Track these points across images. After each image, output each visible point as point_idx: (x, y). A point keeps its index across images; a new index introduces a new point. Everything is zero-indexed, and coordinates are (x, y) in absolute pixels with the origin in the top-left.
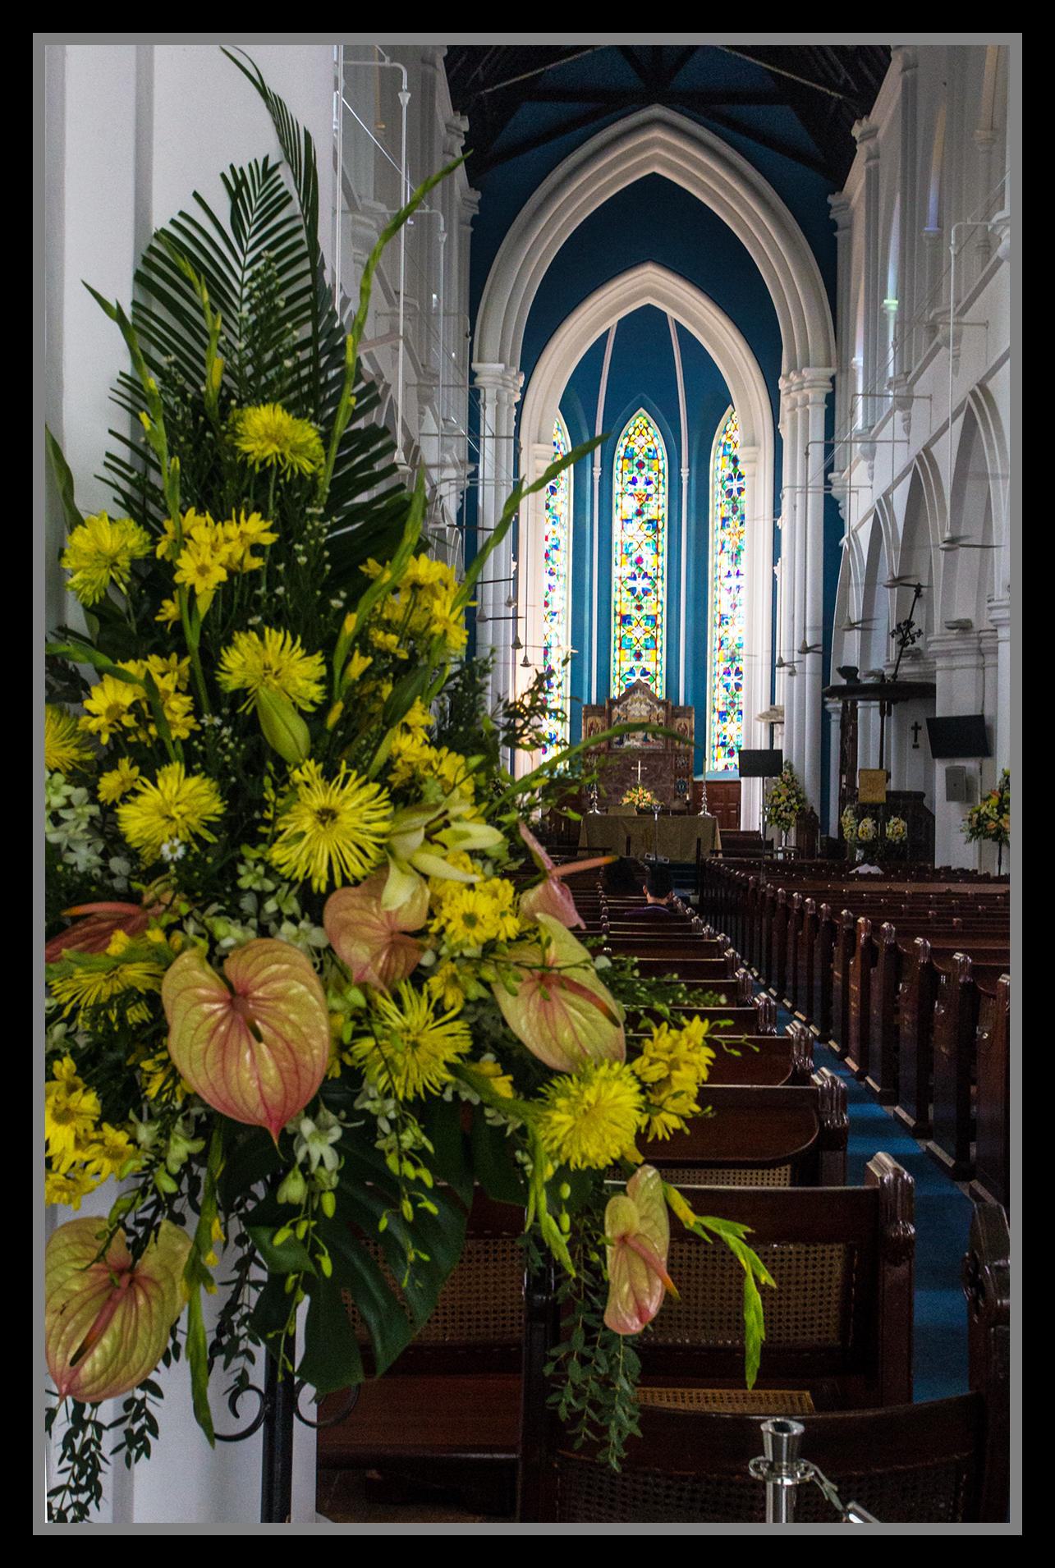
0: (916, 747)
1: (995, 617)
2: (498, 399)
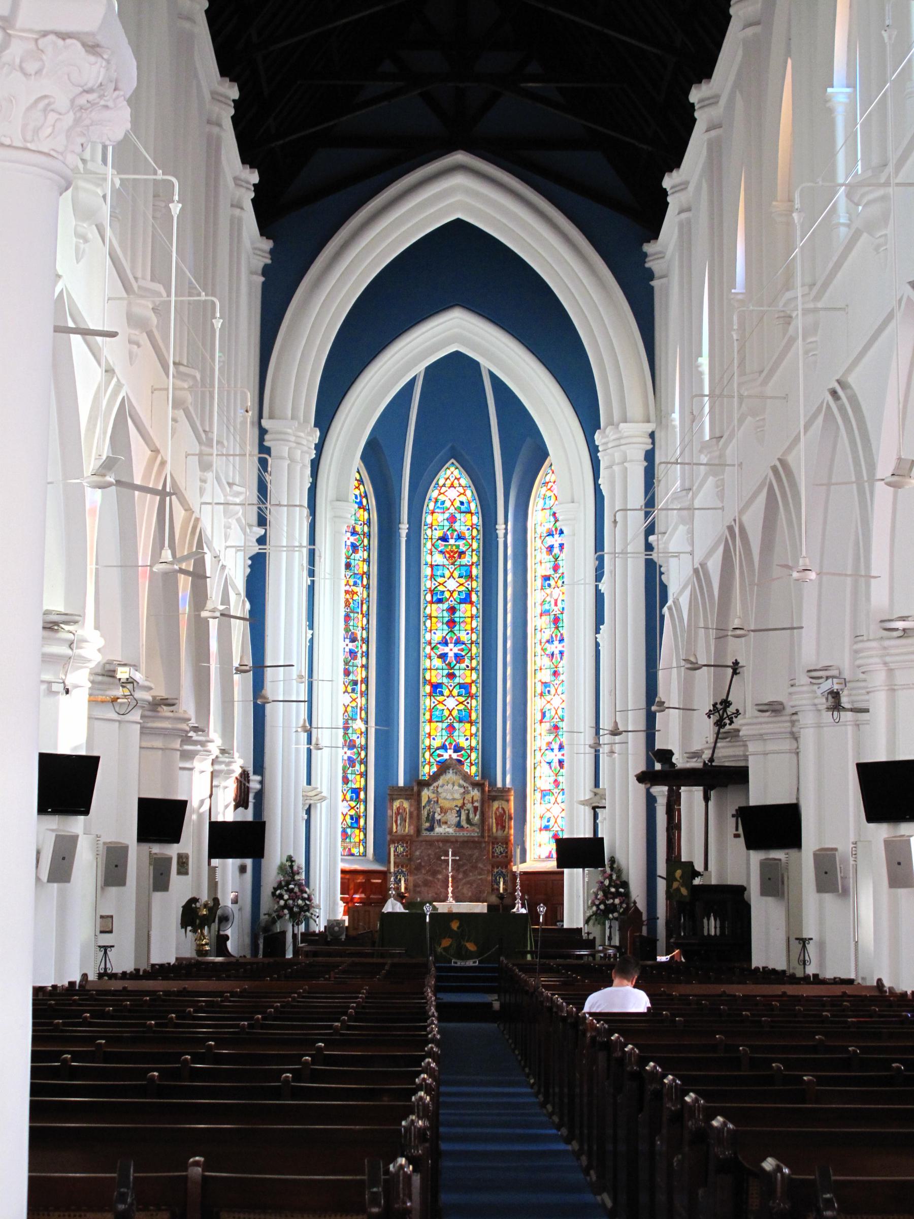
0: (737, 836)
1: (797, 703)
2: (292, 460)
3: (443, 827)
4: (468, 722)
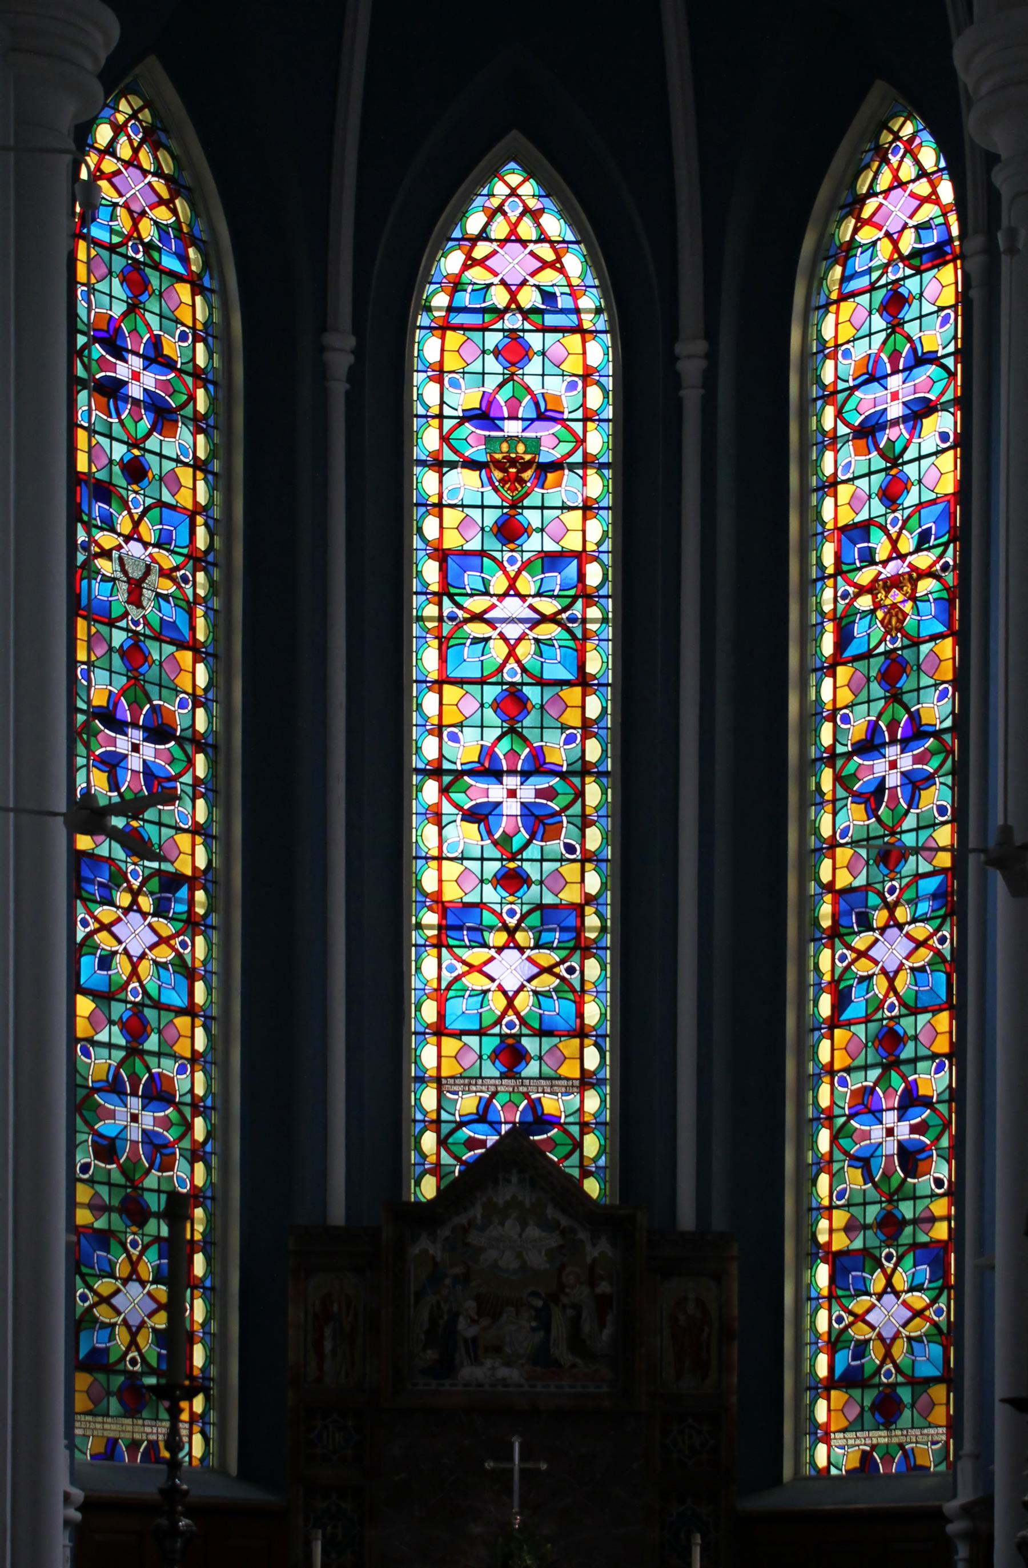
3: (489, 1363)
4: (571, 1034)
